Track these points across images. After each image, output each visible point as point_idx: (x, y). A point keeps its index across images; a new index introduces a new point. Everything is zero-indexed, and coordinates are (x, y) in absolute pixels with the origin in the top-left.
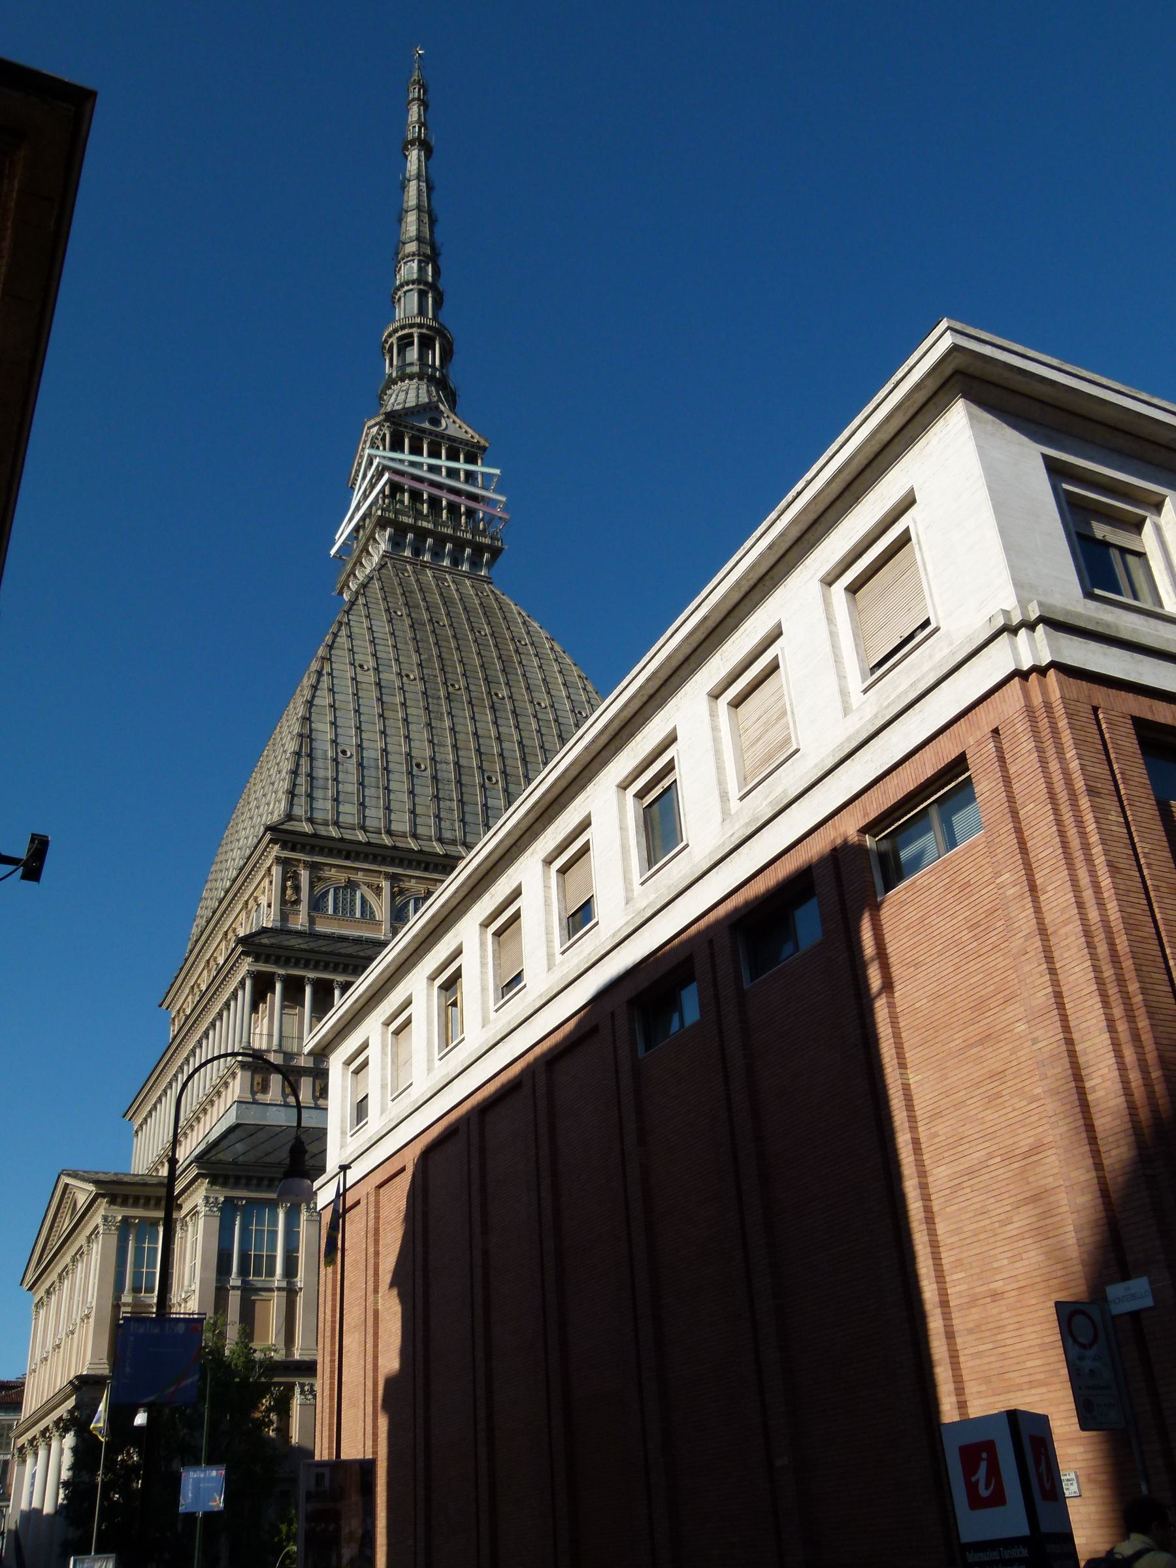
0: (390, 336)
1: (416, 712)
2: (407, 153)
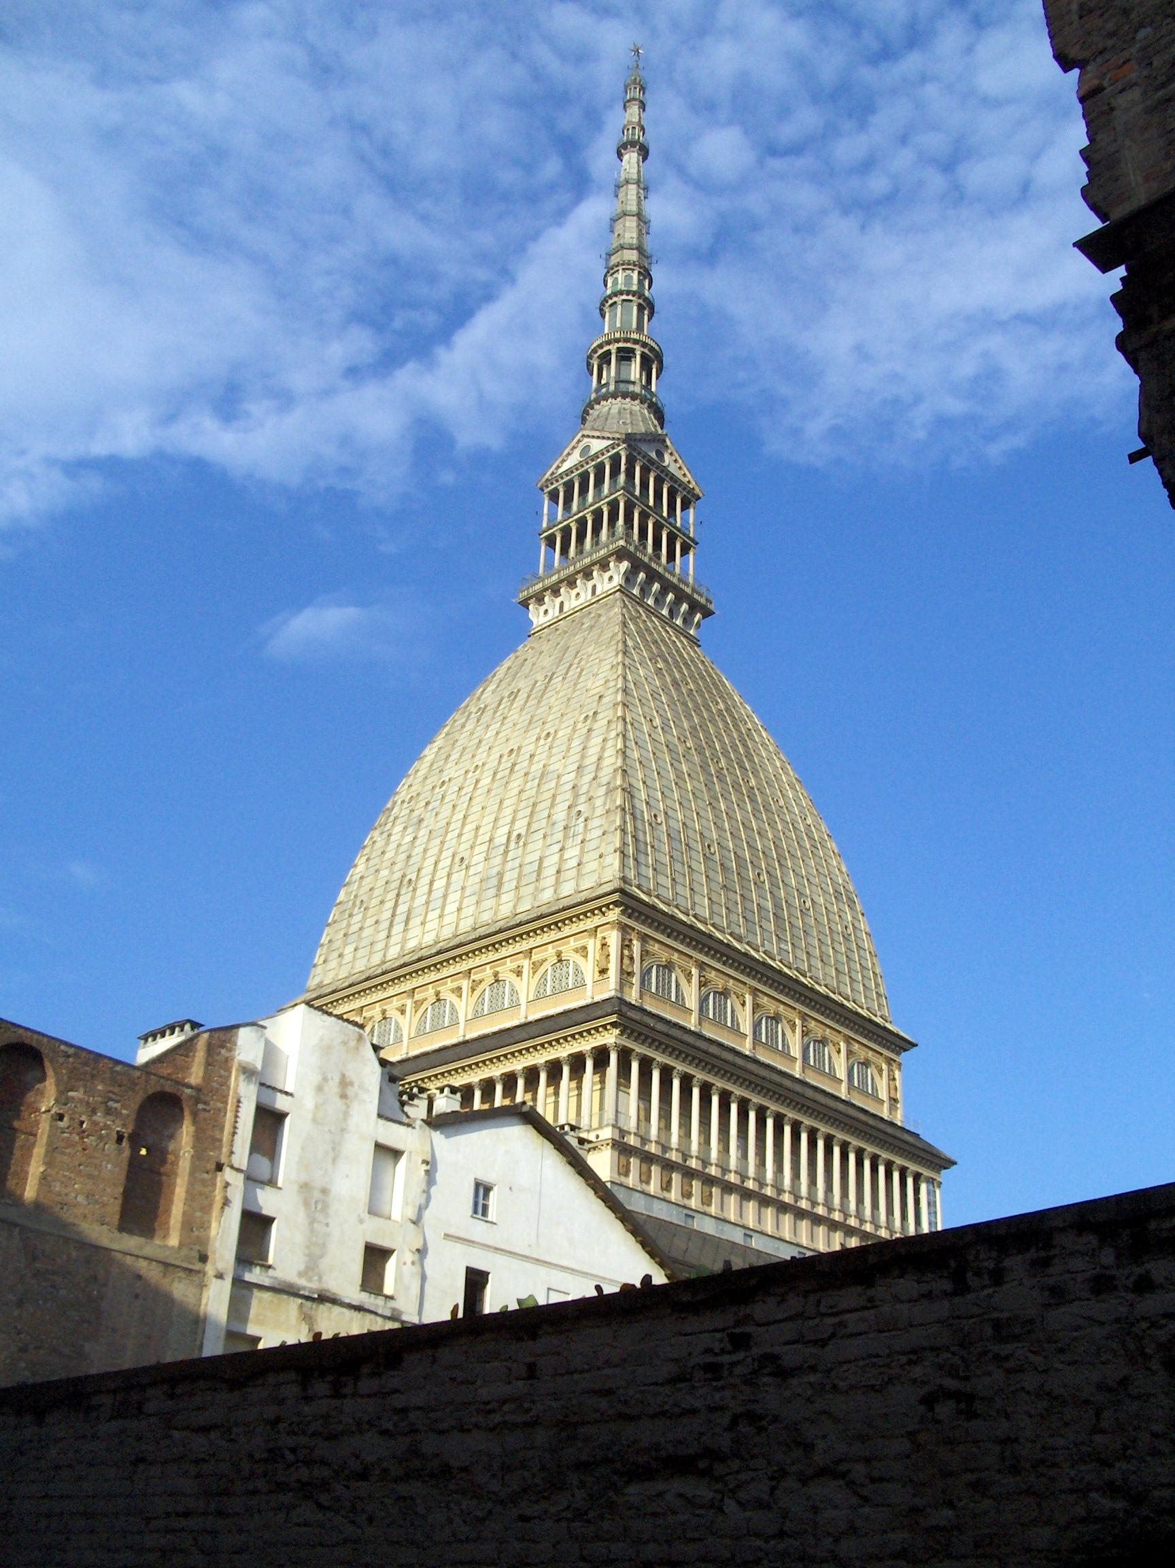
2: (623, 151)
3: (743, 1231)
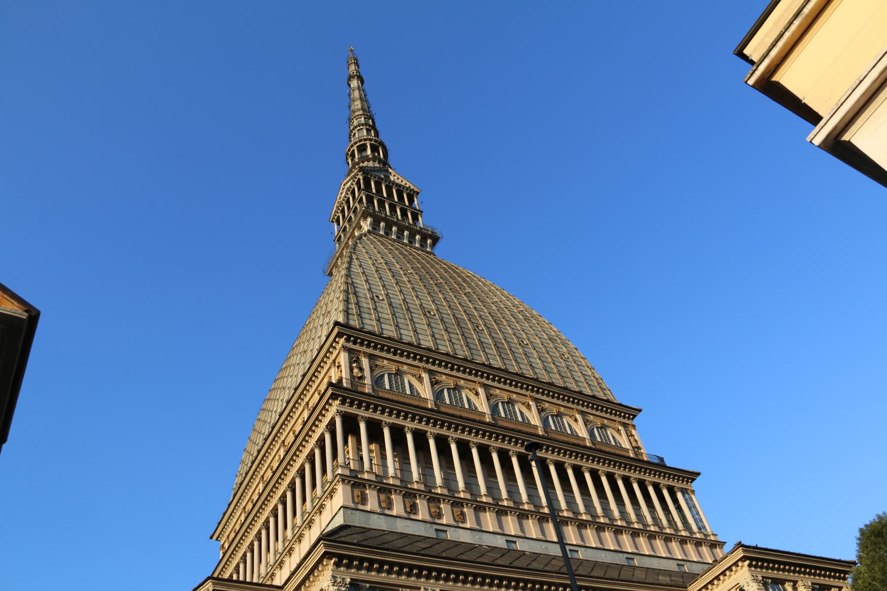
0: (352, 146)
1: (420, 286)
2: (350, 83)
3: (504, 538)
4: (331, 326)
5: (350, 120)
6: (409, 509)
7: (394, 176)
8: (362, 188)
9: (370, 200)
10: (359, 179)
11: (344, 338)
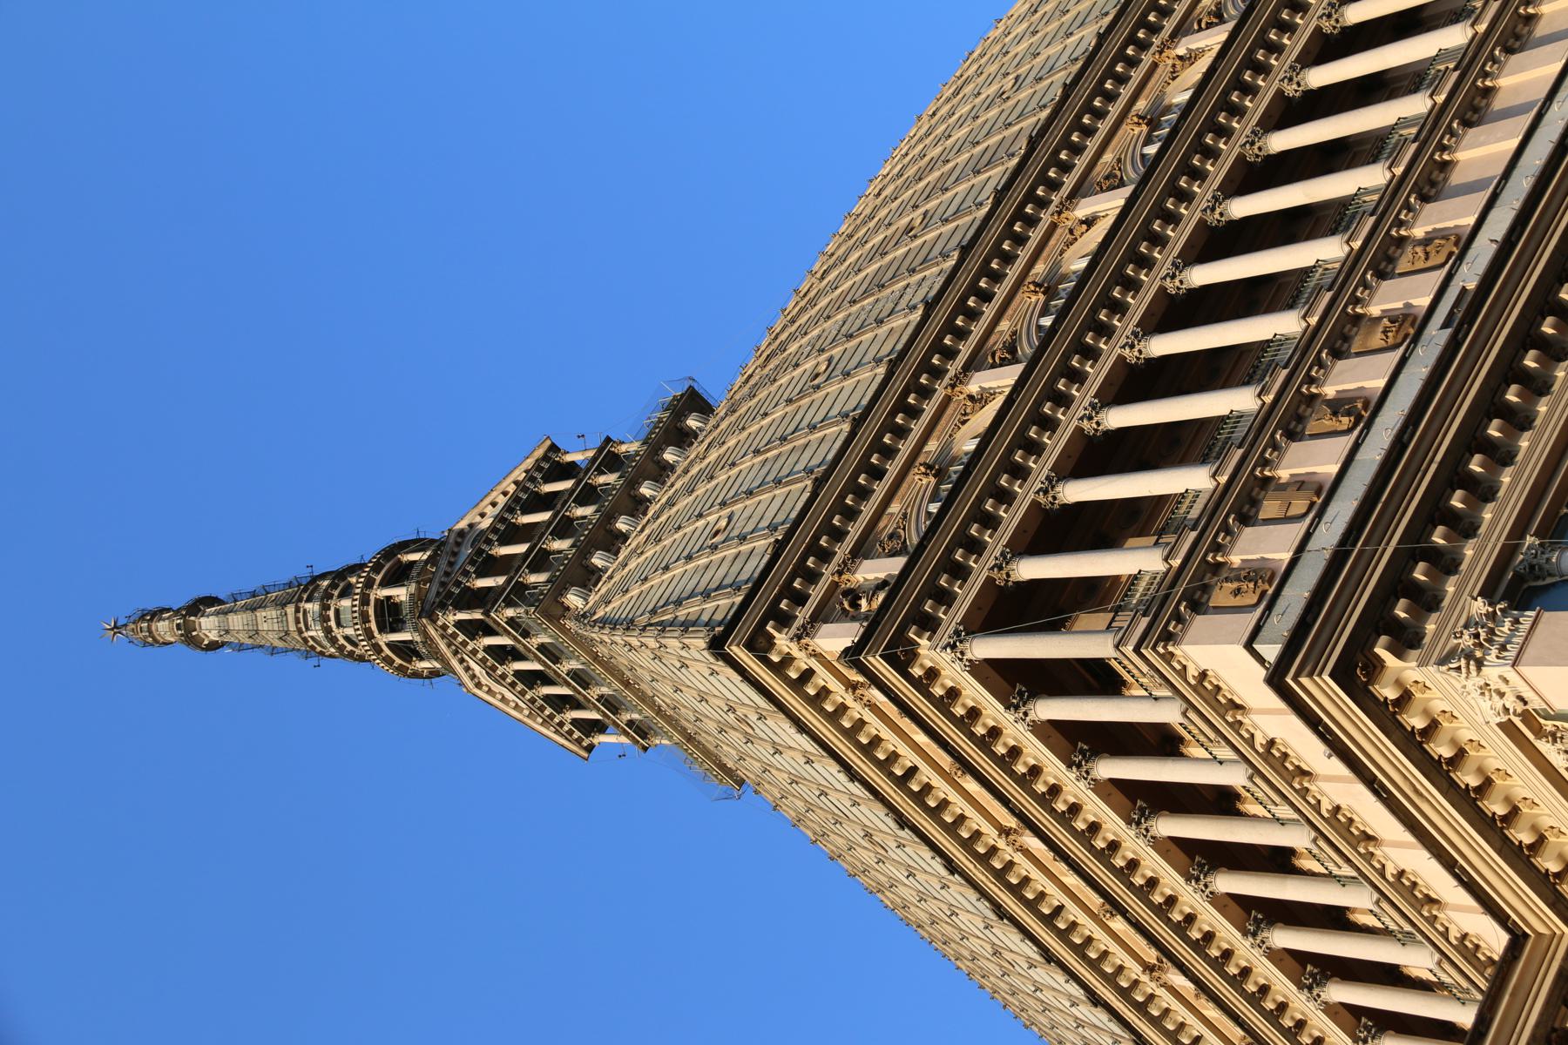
0: (377, 649)
2: (206, 642)
4: (720, 666)
5: (311, 651)
6: (1345, 420)
7: (483, 515)
8: (481, 617)
9: (518, 594)
10: (460, 625)
11: (772, 631)
